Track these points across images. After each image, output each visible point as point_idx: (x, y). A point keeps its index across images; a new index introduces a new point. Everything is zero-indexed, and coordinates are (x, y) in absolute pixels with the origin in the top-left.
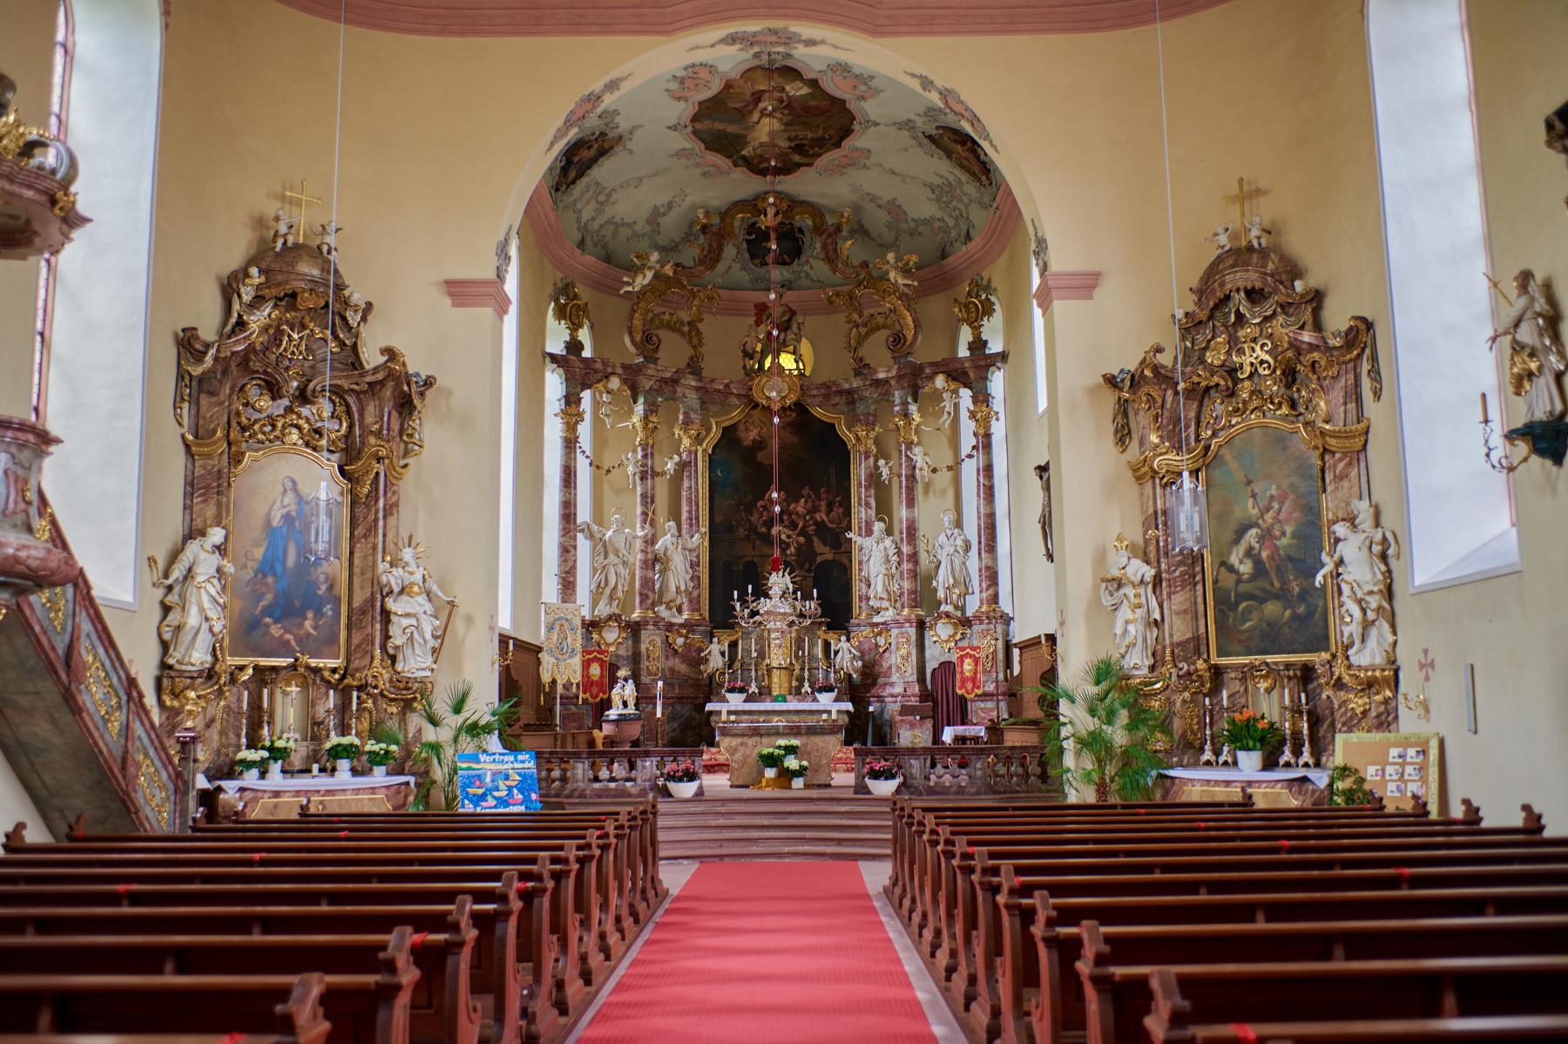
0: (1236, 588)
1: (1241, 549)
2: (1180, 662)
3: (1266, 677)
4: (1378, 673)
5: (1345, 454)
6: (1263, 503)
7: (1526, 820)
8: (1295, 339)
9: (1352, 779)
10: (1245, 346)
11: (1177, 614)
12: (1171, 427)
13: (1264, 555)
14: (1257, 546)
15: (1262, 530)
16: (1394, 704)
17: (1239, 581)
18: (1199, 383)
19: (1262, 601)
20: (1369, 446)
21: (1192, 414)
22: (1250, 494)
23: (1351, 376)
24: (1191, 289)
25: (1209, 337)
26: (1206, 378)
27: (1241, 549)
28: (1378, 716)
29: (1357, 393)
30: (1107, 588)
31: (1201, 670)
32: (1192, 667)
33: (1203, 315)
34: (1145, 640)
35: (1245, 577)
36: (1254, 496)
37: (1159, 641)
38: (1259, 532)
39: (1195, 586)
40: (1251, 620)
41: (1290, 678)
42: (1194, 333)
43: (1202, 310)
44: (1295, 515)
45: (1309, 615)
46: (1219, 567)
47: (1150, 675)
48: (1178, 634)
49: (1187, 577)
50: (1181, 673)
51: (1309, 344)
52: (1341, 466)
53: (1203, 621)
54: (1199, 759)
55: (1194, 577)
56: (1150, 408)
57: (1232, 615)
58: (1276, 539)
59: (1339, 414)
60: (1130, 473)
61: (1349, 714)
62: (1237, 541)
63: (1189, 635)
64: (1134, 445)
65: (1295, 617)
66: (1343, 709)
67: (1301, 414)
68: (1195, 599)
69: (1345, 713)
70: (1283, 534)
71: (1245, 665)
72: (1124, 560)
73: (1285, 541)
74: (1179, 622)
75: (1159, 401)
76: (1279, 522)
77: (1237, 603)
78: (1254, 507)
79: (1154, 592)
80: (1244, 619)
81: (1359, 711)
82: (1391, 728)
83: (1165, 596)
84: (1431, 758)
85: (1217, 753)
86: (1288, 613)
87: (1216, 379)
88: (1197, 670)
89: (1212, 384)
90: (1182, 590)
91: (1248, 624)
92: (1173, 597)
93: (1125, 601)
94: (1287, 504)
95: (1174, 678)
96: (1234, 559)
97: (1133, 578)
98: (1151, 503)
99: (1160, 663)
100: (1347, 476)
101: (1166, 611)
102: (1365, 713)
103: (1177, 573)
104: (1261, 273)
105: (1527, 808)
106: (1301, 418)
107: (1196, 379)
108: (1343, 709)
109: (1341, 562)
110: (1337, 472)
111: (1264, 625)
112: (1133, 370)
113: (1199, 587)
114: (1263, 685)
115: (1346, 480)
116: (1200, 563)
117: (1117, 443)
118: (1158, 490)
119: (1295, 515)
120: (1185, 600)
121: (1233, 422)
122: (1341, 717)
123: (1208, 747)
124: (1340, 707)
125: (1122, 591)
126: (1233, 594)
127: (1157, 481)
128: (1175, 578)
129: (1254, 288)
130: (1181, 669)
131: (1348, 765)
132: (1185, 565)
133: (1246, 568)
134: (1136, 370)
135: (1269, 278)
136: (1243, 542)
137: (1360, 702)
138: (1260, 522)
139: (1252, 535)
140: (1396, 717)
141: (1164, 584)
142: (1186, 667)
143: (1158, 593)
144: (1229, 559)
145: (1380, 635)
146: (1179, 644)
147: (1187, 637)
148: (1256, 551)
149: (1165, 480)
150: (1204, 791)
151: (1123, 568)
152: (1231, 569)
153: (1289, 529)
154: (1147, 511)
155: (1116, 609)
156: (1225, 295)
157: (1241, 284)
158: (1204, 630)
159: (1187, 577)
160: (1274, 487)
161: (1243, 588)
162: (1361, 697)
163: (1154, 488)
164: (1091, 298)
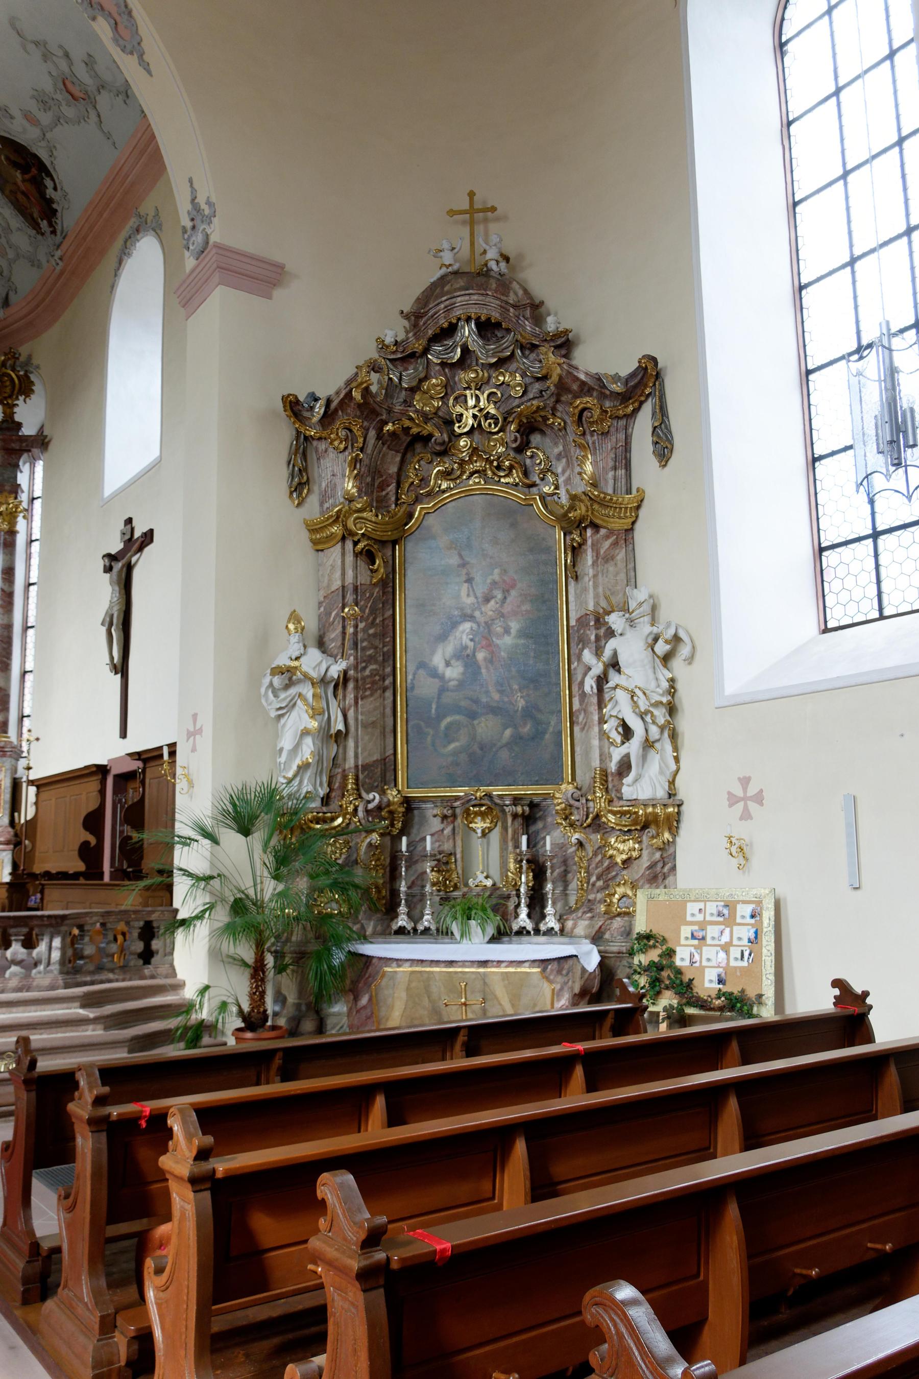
0: (439, 698)
1: (449, 648)
2: (368, 792)
3: (483, 815)
4: (658, 810)
5: (611, 532)
6: (481, 590)
7: (838, 1001)
8: (569, 373)
9: (658, 951)
10: (468, 392)
11: (365, 726)
12: (369, 479)
13: (480, 656)
14: (471, 644)
15: (479, 626)
16: (671, 850)
17: (443, 690)
18: (409, 428)
19: (472, 716)
20: (638, 526)
21: (393, 469)
22: (464, 578)
23: (622, 436)
24: (402, 312)
25: (422, 375)
26: (418, 425)
27: (449, 648)
28: (650, 867)
29: (626, 458)
30: (271, 684)
31: (394, 803)
32: (385, 800)
33: (418, 347)
34: (320, 761)
35: (452, 683)
36: (469, 580)
37: (340, 761)
38: (475, 626)
39: (384, 692)
40: (458, 740)
41: (515, 816)
42: (401, 369)
43: (418, 339)
44: (524, 608)
45: (537, 735)
46: (418, 668)
47: (325, 809)
48: (366, 754)
49: (377, 678)
50: (370, 806)
51: (583, 383)
52: (607, 544)
53: (392, 739)
54: (389, 926)
55: (383, 679)
56: (346, 448)
57: (431, 732)
58: (499, 636)
59: (606, 481)
60: (305, 535)
61: (606, 864)
62: (443, 637)
63: (376, 757)
64: (313, 501)
65: (517, 739)
66: (599, 857)
67: (534, 485)
68: (384, 710)
69: (601, 862)
70: (507, 631)
71: (457, 798)
72: (295, 648)
73: (508, 640)
74: (367, 738)
75: (361, 440)
76: (502, 615)
77: (440, 717)
78: (468, 595)
79: (335, 696)
80: (449, 737)
81: (619, 859)
82: (667, 882)
83: (350, 696)
84: (766, 922)
85: (415, 917)
86: (508, 733)
87: (429, 428)
88: (389, 804)
89: (425, 433)
90: (371, 695)
91: (452, 746)
92: (360, 702)
93: (299, 702)
94: (513, 593)
95: (361, 813)
96: (438, 660)
97: (314, 674)
98: (338, 574)
99: (339, 793)
100: (613, 558)
101: (351, 721)
102: (627, 862)
103: (367, 672)
104: (502, 301)
105: (838, 983)
106: (534, 490)
107: (407, 423)
108: (599, 857)
109: (615, 665)
110: (602, 552)
111: (476, 747)
112: (331, 391)
113: (389, 694)
114: (479, 825)
115: (612, 563)
116: (391, 662)
117: (291, 493)
118: (350, 558)
119: (524, 608)
120: (375, 709)
121: (443, 487)
122: (597, 867)
123: (403, 909)
124: (595, 854)
125: (293, 691)
126: (434, 706)
127: (349, 545)
128: (364, 679)
129: (489, 319)
130: (369, 802)
131: (654, 932)
132: (376, 662)
133: (453, 673)
134: (337, 393)
135: (511, 310)
136: (451, 638)
137: (621, 846)
138: (477, 614)
139: (464, 632)
140: (674, 868)
141: (351, 685)
142: (377, 797)
143: (340, 696)
144: (431, 660)
145: (663, 760)
146: (365, 767)
147: (375, 759)
148: (468, 651)
149: (360, 546)
150: (413, 972)
151: (297, 659)
152: (434, 673)
153: (514, 626)
154: (328, 586)
155: (280, 717)
156: (450, 323)
157: (473, 311)
158: (391, 752)
159: (377, 678)
160: (497, 571)
161: (447, 698)
162: (624, 841)
163: (343, 554)
164: (269, 297)
